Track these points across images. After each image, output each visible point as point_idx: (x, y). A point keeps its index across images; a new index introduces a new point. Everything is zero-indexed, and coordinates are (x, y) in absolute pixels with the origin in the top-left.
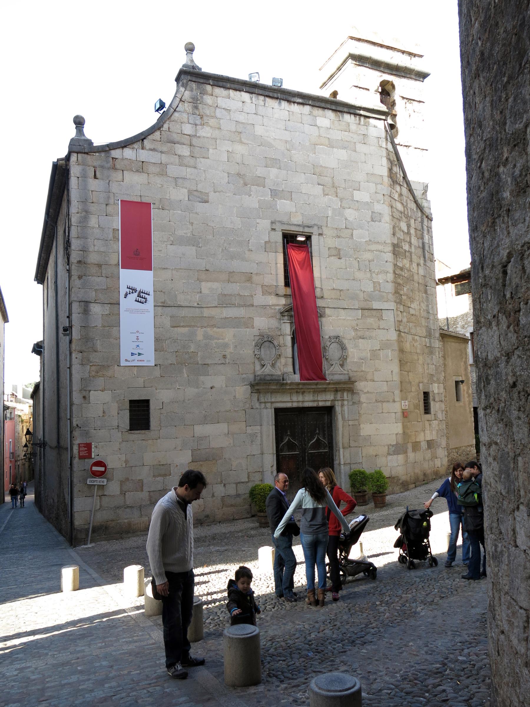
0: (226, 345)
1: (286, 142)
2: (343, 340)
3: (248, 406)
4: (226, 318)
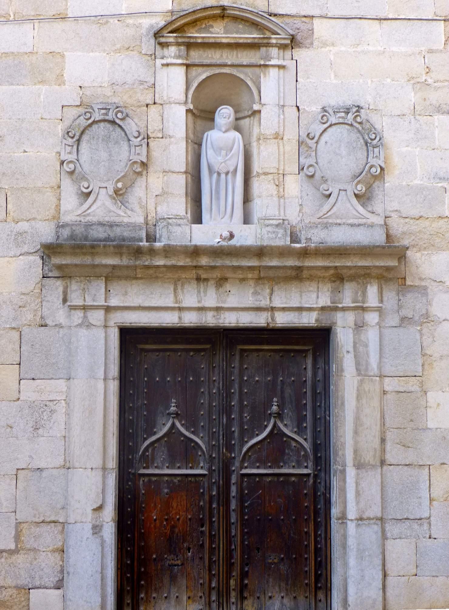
2: (375, 119)
3: (30, 316)
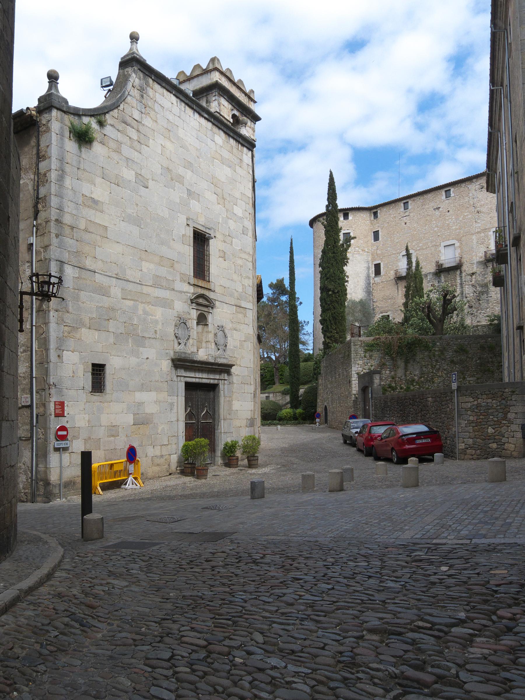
0: (157, 322)
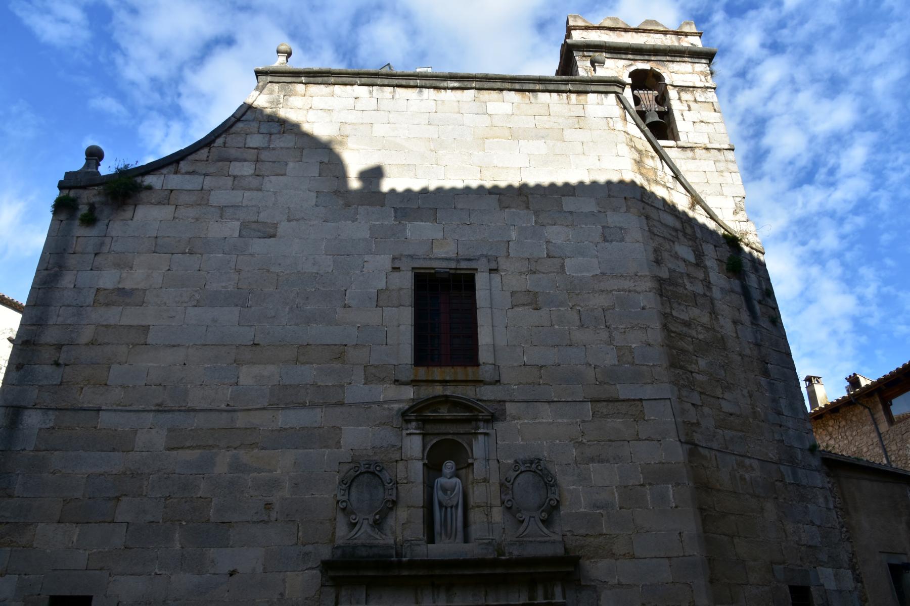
1: (429, 140)
4: (281, 430)
